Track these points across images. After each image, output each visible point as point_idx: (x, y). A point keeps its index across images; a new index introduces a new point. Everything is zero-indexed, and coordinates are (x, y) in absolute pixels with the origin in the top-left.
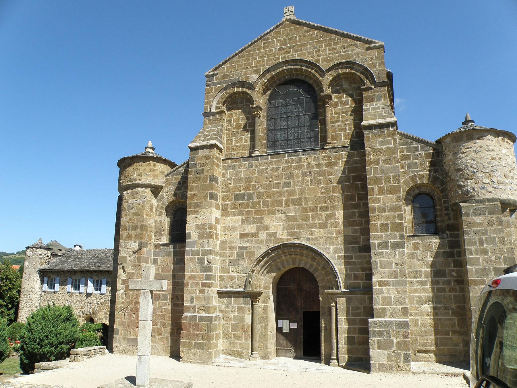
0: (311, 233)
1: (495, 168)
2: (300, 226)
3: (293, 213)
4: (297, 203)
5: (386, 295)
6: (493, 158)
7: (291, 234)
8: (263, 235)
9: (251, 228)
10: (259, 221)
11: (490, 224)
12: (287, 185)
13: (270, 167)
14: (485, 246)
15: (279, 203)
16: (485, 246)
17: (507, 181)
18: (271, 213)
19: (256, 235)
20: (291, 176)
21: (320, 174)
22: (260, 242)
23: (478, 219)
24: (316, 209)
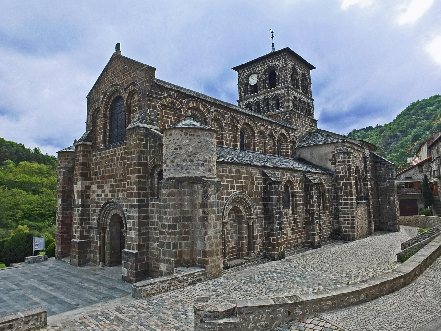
0: (118, 195)
1: (176, 155)
2: (115, 192)
3: (113, 183)
4: (114, 176)
5: (131, 236)
6: (176, 149)
7: (113, 195)
8: (103, 196)
9: (100, 192)
10: (102, 187)
11: (169, 195)
12: (111, 166)
13: (106, 155)
14: (166, 210)
15: (108, 177)
16: (166, 210)
17: (184, 164)
18: (106, 183)
19: (101, 195)
20: (112, 160)
21: (122, 159)
22: (102, 199)
23: (164, 192)
24: (119, 181)
